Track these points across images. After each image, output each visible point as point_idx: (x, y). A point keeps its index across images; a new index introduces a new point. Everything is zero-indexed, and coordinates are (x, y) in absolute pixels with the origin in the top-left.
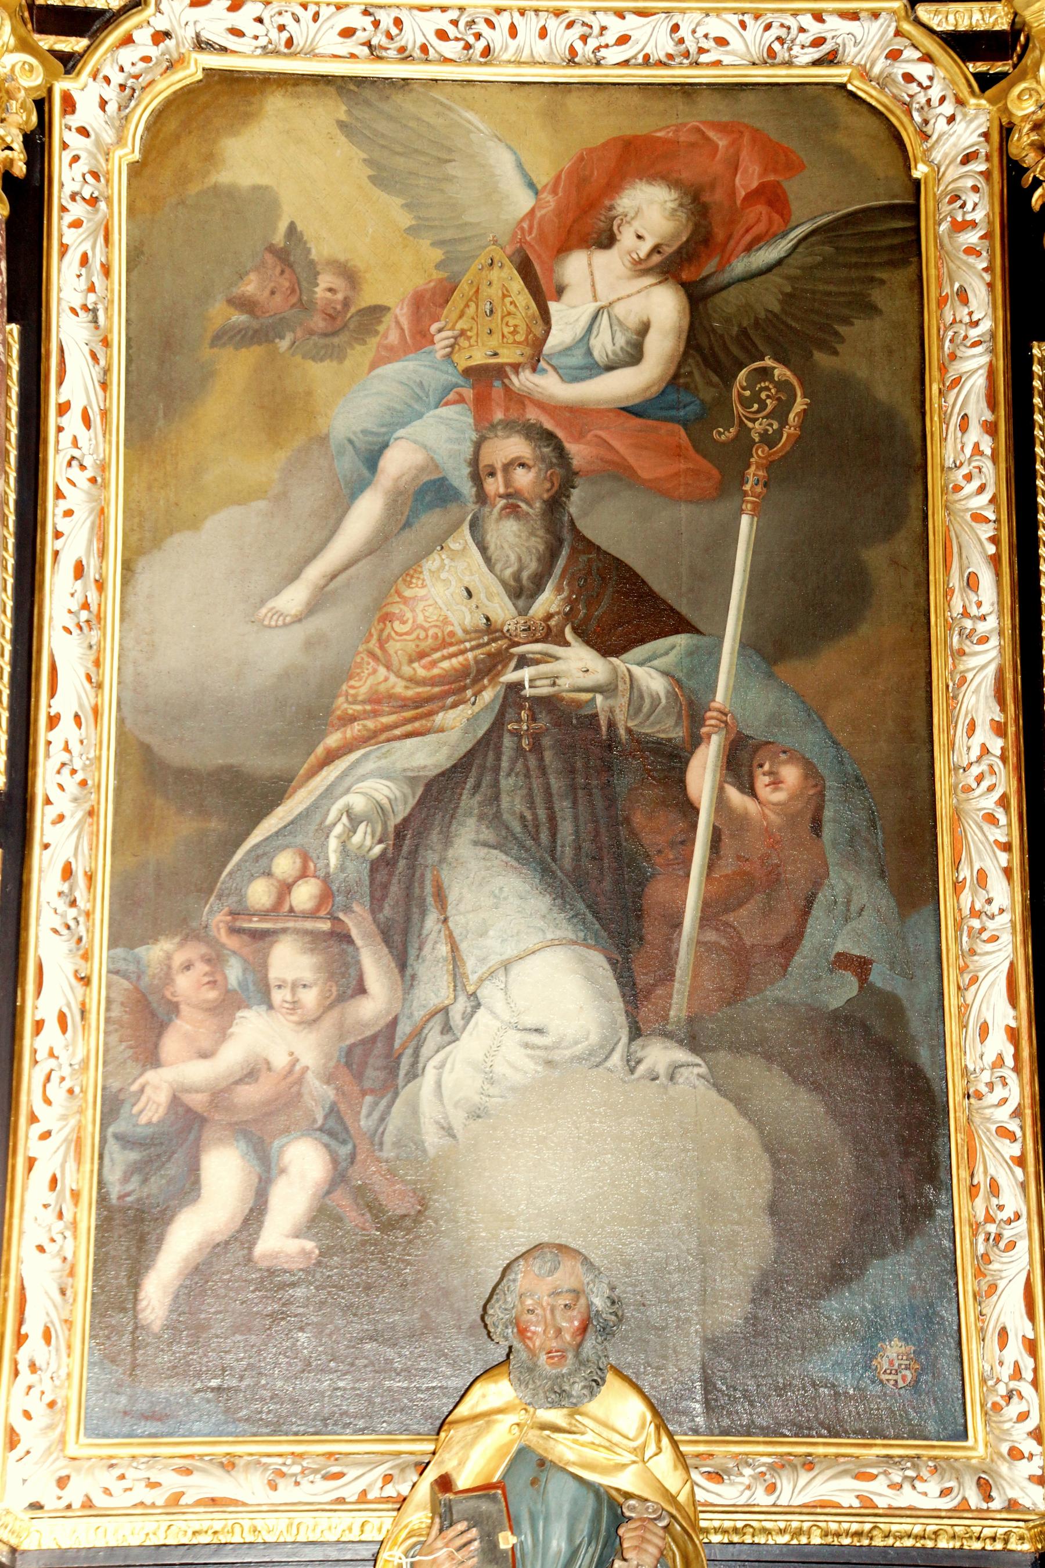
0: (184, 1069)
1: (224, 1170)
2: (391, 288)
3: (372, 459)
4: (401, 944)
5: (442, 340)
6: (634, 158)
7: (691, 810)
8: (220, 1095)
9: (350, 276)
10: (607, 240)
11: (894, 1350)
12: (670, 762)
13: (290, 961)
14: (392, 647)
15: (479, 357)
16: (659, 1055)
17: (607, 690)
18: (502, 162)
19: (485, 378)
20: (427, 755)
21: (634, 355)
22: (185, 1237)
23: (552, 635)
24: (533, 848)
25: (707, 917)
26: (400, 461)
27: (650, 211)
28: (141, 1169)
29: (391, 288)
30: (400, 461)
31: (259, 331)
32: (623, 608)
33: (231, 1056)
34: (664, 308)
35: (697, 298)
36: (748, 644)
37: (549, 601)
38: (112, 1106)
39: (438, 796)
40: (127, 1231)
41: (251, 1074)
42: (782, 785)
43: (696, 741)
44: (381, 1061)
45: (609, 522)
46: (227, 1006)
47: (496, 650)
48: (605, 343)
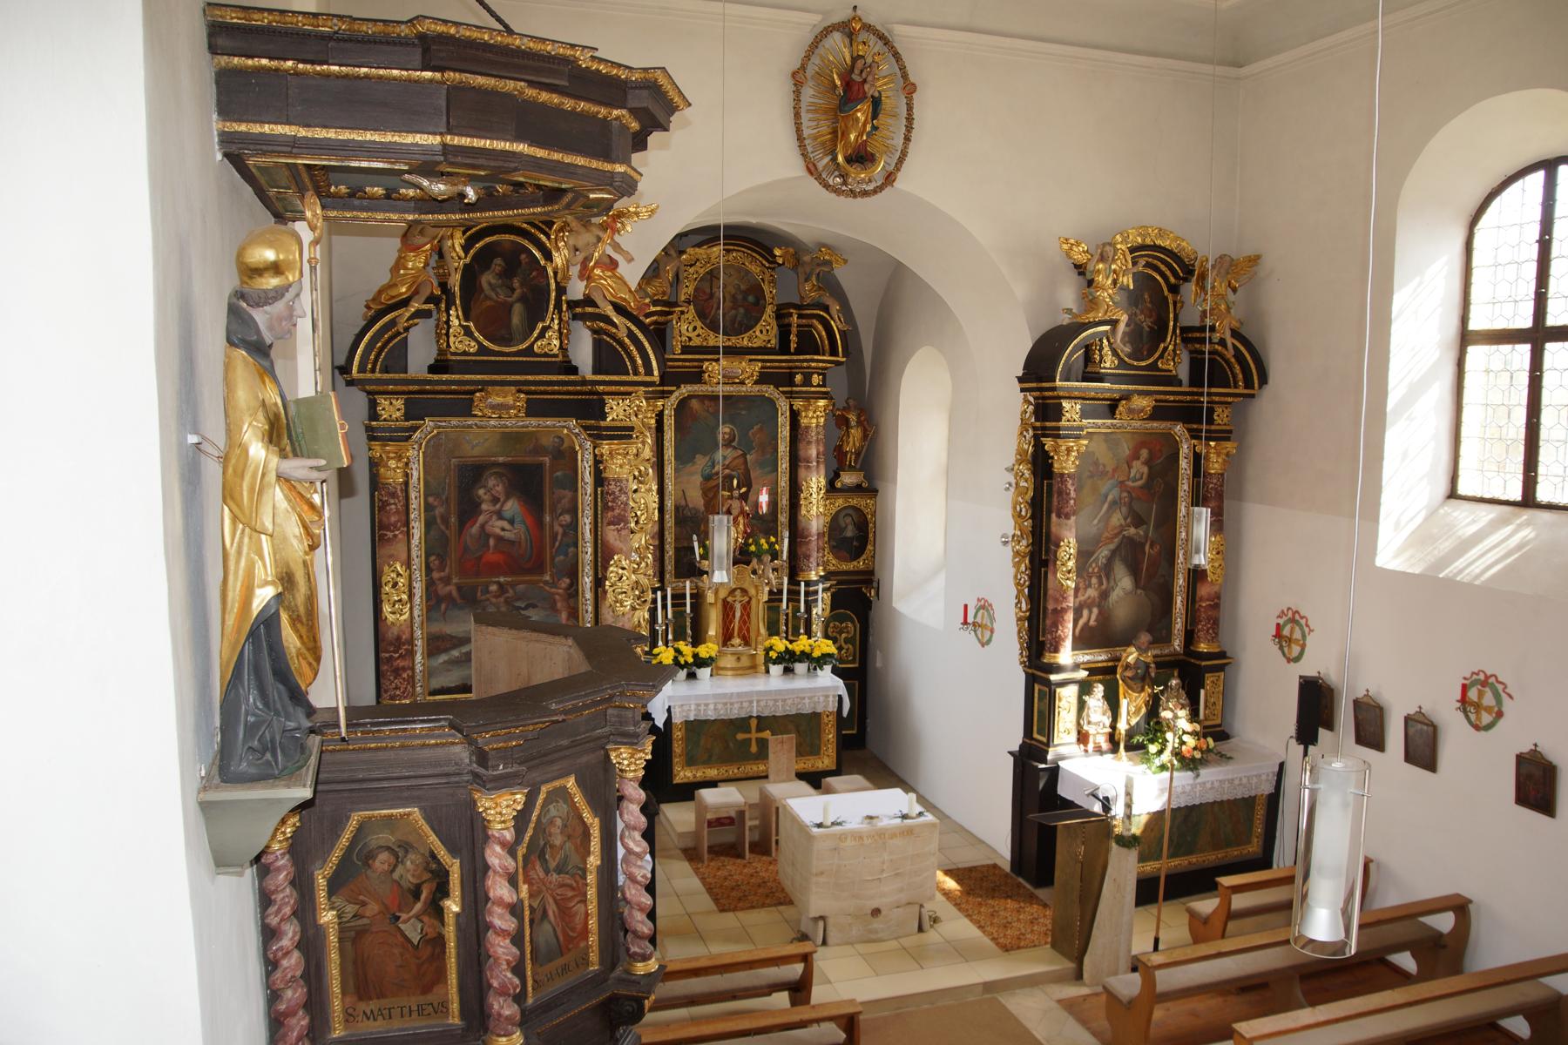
1: (1085, 613)
6: (1142, 445)
12: (1143, 545)
13: (1094, 580)
20: (1112, 546)
22: (1081, 623)
24: (1125, 561)
26: (1110, 497)
27: (1144, 453)
29: (1109, 469)
30: (1110, 497)
31: (1091, 477)
32: (1138, 521)
34: (1145, 470)
35: (1150, 468)
39: (1114, 553)
44: (1104, 595)
45: (1136, 506)
47: (1122, 528)
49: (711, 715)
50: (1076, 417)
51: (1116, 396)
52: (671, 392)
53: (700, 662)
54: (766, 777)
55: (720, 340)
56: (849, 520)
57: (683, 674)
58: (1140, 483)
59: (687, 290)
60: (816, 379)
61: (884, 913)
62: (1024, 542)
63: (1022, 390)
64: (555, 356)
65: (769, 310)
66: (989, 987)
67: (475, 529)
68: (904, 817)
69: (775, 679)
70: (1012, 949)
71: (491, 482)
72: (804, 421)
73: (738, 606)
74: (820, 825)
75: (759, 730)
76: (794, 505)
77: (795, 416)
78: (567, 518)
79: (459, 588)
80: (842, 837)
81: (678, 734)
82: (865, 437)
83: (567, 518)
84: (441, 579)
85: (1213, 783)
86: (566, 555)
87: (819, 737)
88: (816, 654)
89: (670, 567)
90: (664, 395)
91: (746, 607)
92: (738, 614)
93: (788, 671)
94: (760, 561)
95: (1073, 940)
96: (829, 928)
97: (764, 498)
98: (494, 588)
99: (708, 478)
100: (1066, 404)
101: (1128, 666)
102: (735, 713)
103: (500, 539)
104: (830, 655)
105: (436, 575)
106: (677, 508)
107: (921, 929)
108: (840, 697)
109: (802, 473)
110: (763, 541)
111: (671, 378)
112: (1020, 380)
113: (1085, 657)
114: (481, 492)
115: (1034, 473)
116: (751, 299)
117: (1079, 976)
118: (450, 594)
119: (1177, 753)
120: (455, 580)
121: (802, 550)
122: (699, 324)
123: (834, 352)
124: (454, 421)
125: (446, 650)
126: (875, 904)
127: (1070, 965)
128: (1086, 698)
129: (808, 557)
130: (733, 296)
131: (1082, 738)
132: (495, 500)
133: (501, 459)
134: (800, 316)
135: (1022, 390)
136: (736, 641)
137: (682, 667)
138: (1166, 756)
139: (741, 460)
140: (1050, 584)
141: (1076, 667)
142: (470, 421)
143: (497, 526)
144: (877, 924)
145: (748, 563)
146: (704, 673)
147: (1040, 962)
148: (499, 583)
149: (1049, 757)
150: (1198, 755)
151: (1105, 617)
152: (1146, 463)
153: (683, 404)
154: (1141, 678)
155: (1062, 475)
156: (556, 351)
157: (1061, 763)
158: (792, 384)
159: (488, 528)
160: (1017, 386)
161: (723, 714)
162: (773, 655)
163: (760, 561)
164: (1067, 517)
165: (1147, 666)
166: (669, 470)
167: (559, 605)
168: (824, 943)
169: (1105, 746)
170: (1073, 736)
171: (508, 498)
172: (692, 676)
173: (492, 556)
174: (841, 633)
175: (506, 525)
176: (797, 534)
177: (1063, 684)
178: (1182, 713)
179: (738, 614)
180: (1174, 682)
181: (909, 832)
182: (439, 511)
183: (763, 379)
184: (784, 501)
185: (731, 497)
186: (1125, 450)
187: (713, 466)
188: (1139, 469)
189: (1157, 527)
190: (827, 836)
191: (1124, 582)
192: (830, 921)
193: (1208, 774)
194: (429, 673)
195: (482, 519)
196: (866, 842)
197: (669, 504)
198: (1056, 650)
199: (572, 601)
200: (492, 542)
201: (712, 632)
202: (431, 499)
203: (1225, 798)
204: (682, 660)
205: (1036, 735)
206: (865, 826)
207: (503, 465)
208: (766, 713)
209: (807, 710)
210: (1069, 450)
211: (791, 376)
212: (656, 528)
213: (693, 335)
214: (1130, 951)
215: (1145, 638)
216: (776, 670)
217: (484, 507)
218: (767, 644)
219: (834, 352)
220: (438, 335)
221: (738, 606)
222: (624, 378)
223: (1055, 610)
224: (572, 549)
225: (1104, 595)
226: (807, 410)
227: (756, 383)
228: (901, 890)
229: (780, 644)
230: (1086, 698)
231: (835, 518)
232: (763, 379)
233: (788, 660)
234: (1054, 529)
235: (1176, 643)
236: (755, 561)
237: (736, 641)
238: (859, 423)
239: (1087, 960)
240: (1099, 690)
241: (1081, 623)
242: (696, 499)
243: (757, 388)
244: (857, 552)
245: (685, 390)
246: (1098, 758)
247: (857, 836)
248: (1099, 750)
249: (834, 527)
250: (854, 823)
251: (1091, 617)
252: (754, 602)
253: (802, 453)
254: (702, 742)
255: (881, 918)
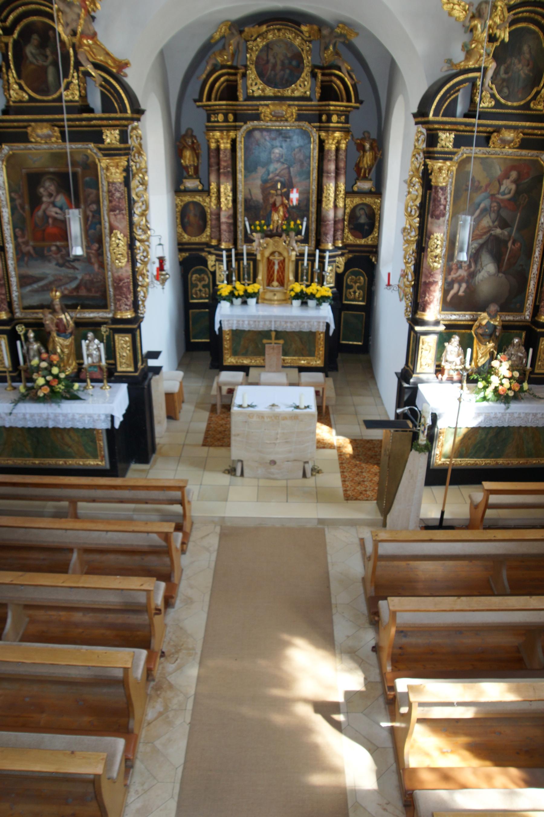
0: (453, 275)
1: (456, 286)
2: (483, 184)
3: (479, 205)
4: (476, 263)
5: (488, 190)
6: (513, 168)
7: (508, 248)
8: (456, 278)
9: (479, 182)
10: (508, 178)
11: (518, 305)
12: (506, 242)
14: (480, 229)
15: (492, 193)
16: (500, 275)
17: (501, 234)
18: (498, 168)
19: (492, 196)
20: (481, 241)
21: (509, 193)
22: (452, 293)
23: (496, 227)
25: (508, 259)
26: (482, 206)
27: (514, 175)
28: (448, 286)
29: (483, 184)
30: (482, 206)
32: (504, 224)
33: (458, 274)
34: (513, 187)
35: (517, 186)
36: (517, 229)
37: (496, 223)
38: (445, 279)
39: (481, 246)
40: (446, 292)
41: (460, 276)
42: (518, 245)
43: (509, 240)
44: (472, 275)
45: (504, 214)
46: (457, 269)
47: (490, 229)
48: (506, 191)
49: (246, 327)
50: (450, 145)
51: (489, 129)
52: (241, 127)
53: (247, 295)
54: (264, 367)
55: (270, 91)
56: (362, 212)
57: (239, 300)
58: (507, 197)
59: (252, 56)
60: (335, 118)
61: (278, 463)
62: (413, 234)
63: (417, 123)
64: (76, 102)
65: (307, 70)
66: (321, 521)
67: (40, 213)
68: (297, 407)
69: (295, 309)
70: (352, 499)
71: (47, 184)
72: (327, 147)
73: (276, 262)
74: (240, 406)
75: (277, 338)
76: (319, 201)
77: (322, 142)
78: (94, 207)
79: (34, 248)
80: (250, 415)
81: (227, 337)
82: (375, 158)
83: (94, 207)
84: (24, 243)
85: (521, 413)
86: (95, 229)
87: (315, 347)
88: (318, 295)
89: (240, 236)
90: (236, 128)
91: (282, 263)
92: (276, 267)
93: (304, 304)
94: (288, 235)
95: (386, 499)
96: (245, 468)
97: (294, 196)
98: (54, 248)
99: (265, 182)
100: (443, 135)
101: (480, 326)
102: (261, 327)
103: (55, 219)
104: (328, 297)
105: (20, 240)
106: (246, 201)
107: (304, 475)
108: (328, 326)
109: (325, 180)
110: (292, 223)
111: (240, 117)
112: (415, 116)
113: (455, 316)
114: (42, 190)
115: (423, 185)
116: (294, 63)
117: (384, 525)
118: (29, 253)
119: (496, 390)
120: (31, 243)
121: (323, 229)
122: (259, 81)
123: (349, 100)
124: (22, 146)
125: (30, 284)
126: (272, 457)
127: (380, 517)
128: (446, 344)
129: (326, 234)
130: (283, 63)
131: (439, 370)
132: (50, 195)
133: (52, 170)
134: (323, 75)
135: (417, 123)
136: (275, 283)
137: (237, 297)
138: (489, 393)
139: (286, 171)
140: (424, 265)
141: (437, 323)
142: (30, 146)
143: (53, 211)
144: (273, 469)
145: (280, 236)
146: (252, 302)
147: (367, 510)
148: (56, 246)
149: (412, 380)
150: (511, 394)
151: (471, 291)
152: (515, 182)
153: (250, 133)
154: (489, 334)
155: (436, 187)
156: (77, 98)
157: (420, 386)
158: (320, 121)
159: (48, 213)
160: (412, 121)
161: (253, 327)
162: (293, 294)
163: (288, 235)
164: (438, 218)
165: (495, 327)
166: (240, 177)
167: (93, 260)
168: (242, 474)
169: (456, 377)
170: (432, 369)
171: (58, 193)
172: (245, 303)
173: (51, 230)
174: (355, 282)
175: (58, 211)
176: (320, 219)
177: (426, 333)
178: (506, 365)
179: (276, 267)
180: (516, 341)
181: (295, 417)
182: (18, 202)
183: (300, 118)
184: (314, 198)
185: (277, 195)
186: (498, 171)
187: (269, 174)
188: (508, 186)
189: (518, 230)
190: (241, 414)
191: (489, 267)
192: (245, 463)
193: (516, 407)
194: (22, 297)
195: (43, 206)
196: (266, 420)
197: (240, 197)
198: (424, 310)
199: (100, 258)
200: (50, 221)
201: (260, 277)
202: (13, 195)
203: (529, 425)
204: (236, 293)
205: (410, 364)
206: (268, 410)
207: (54, 173)
208: (280, 329)
209: (306, 328)
210: (440, 169)
211: (320, 116)
212: (231, 212)
213: (255, 88)
214: (418, 516)
215: (493, 308)
216: (296, 303)
217: (45, 199)
218: (290, 287)
219: (349, 100)
220: (4, 91)
221: (276, 262)
222: (113, 115)
223: (425, 283)
224: (98, 226)
225: (472, 275)
226: (328, 139)
227: (296, 120)
228: (290, 452)
229: (298, 287)
230: (446, 344)
231: (353, 210)
232: (300, 118)
233: (303, 298)
234: (429, 226)
235: (527, 313)
236: (284, 236)
237: (275, 283)
238: (372, 148)
239: (388, 516)
240: (456, 340)
241: (452, 293)
242: (257, 195)
243: (297, 123)
244: (365, 235)
245: (250, 124)
246: (449, 385)
247: (261, 416)
248: (451, 380)
249: (353, 216)
250: (262, 407)
251: (459, 289)
252: (286, 260)
253: (325, 168)
254: (242, 343)
255: (275, 466)
